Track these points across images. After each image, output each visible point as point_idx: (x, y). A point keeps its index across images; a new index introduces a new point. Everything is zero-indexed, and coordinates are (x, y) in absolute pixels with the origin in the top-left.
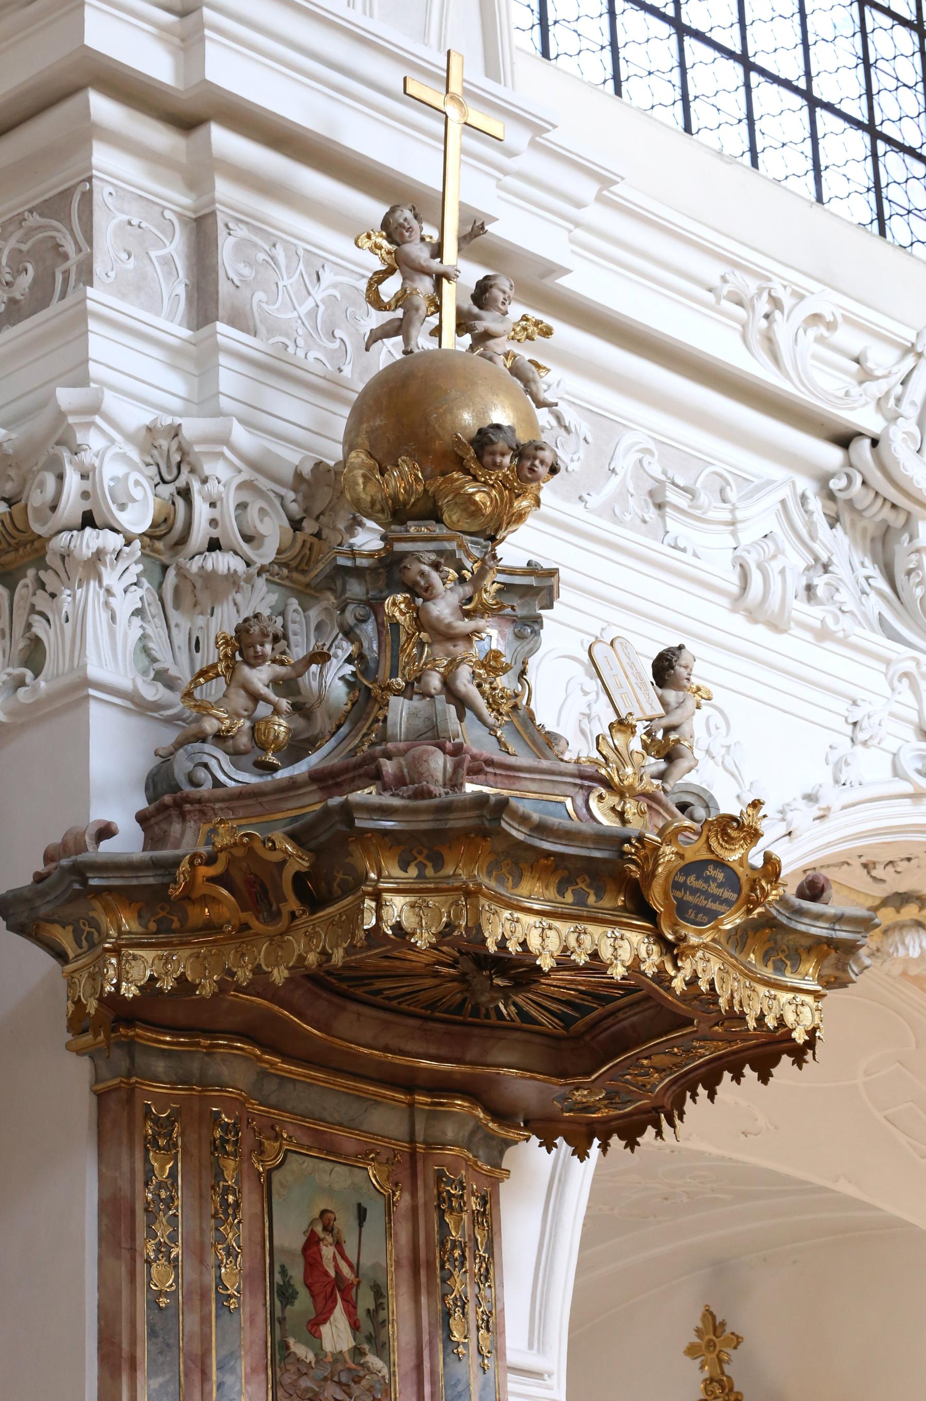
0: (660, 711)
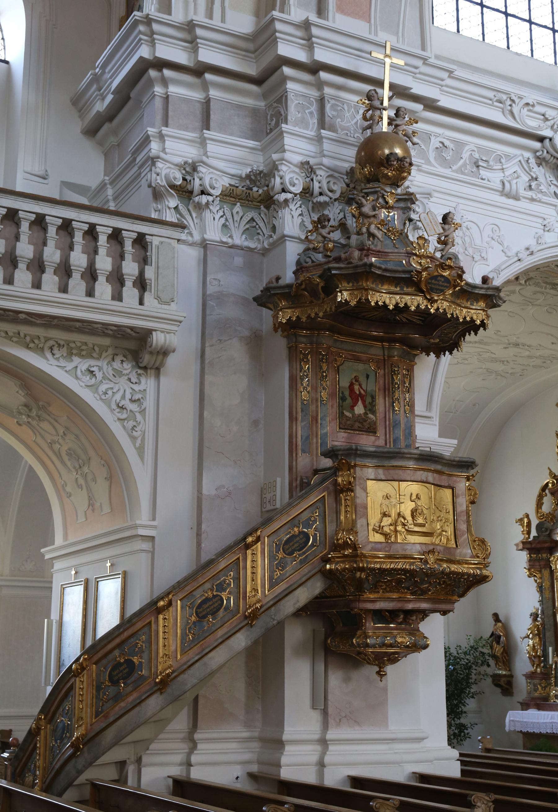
0: (442, 231)
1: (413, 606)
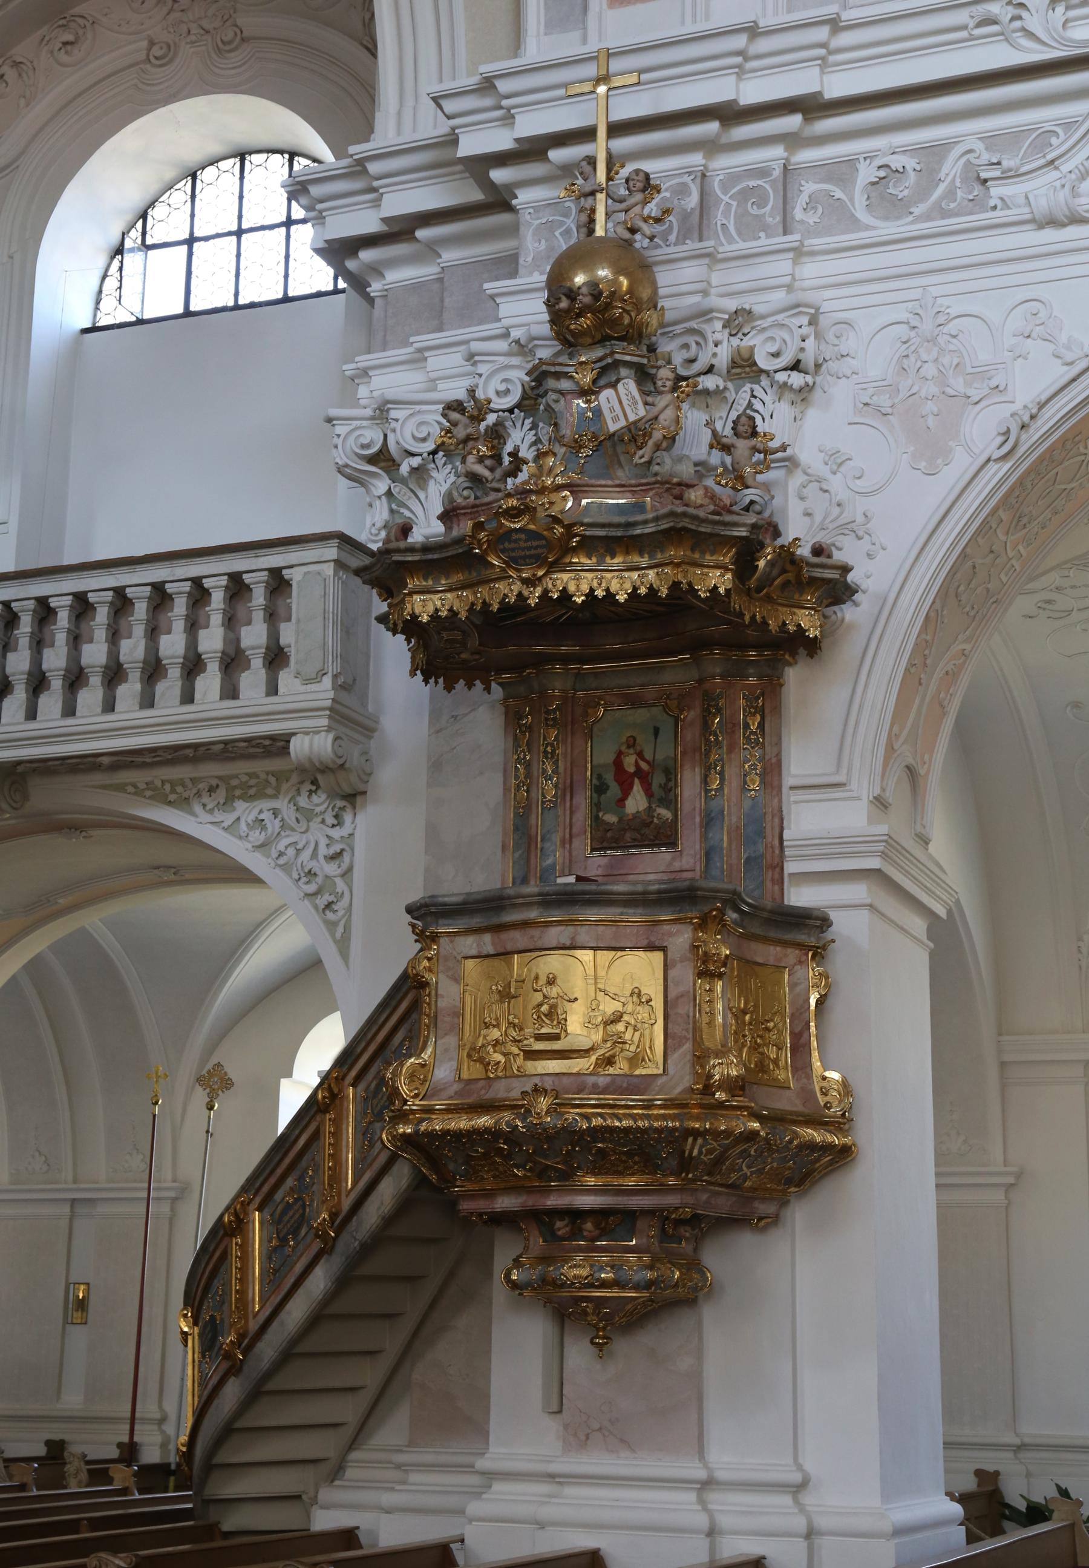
1: (554, 1203)
